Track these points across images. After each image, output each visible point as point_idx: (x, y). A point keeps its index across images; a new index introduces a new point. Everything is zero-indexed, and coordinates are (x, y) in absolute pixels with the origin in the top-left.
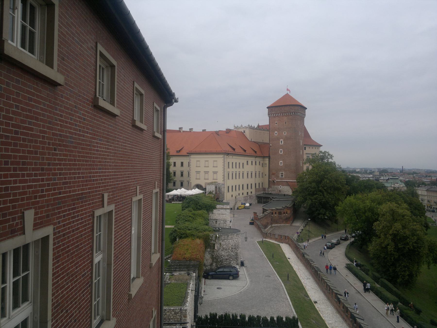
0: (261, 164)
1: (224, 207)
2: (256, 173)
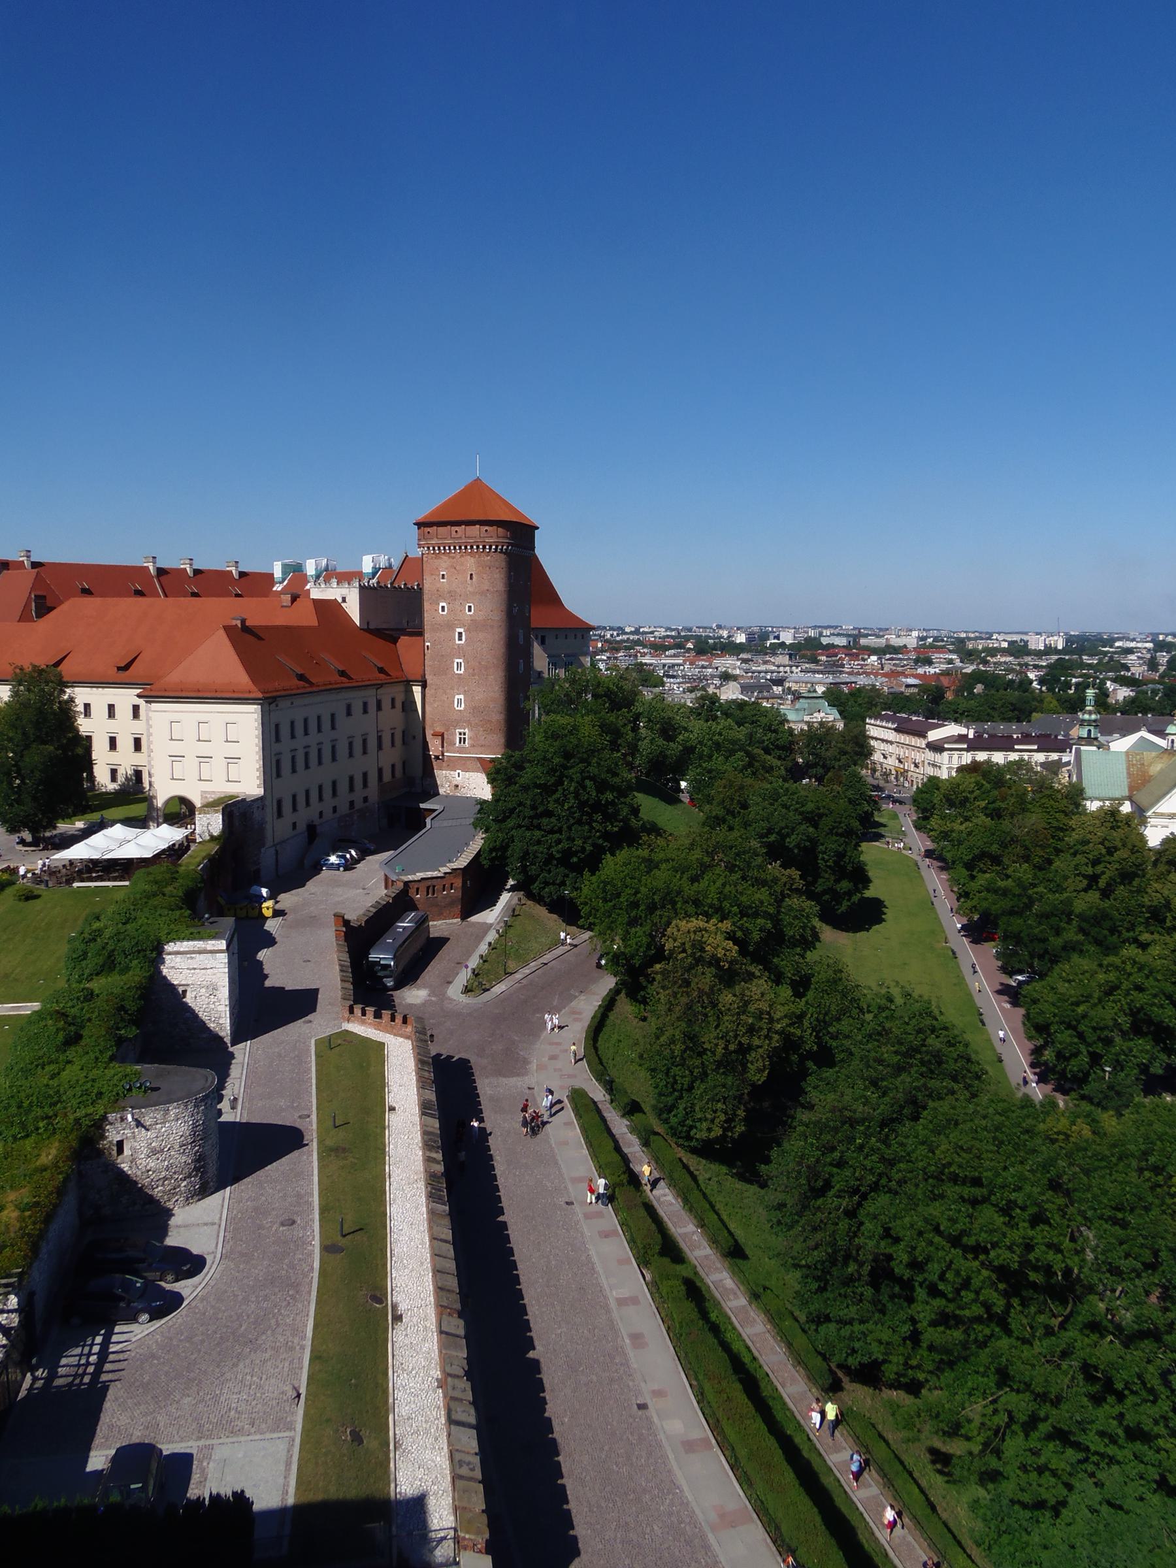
0: (399, 704)
1: (209, 948)
2: (380, 738)
